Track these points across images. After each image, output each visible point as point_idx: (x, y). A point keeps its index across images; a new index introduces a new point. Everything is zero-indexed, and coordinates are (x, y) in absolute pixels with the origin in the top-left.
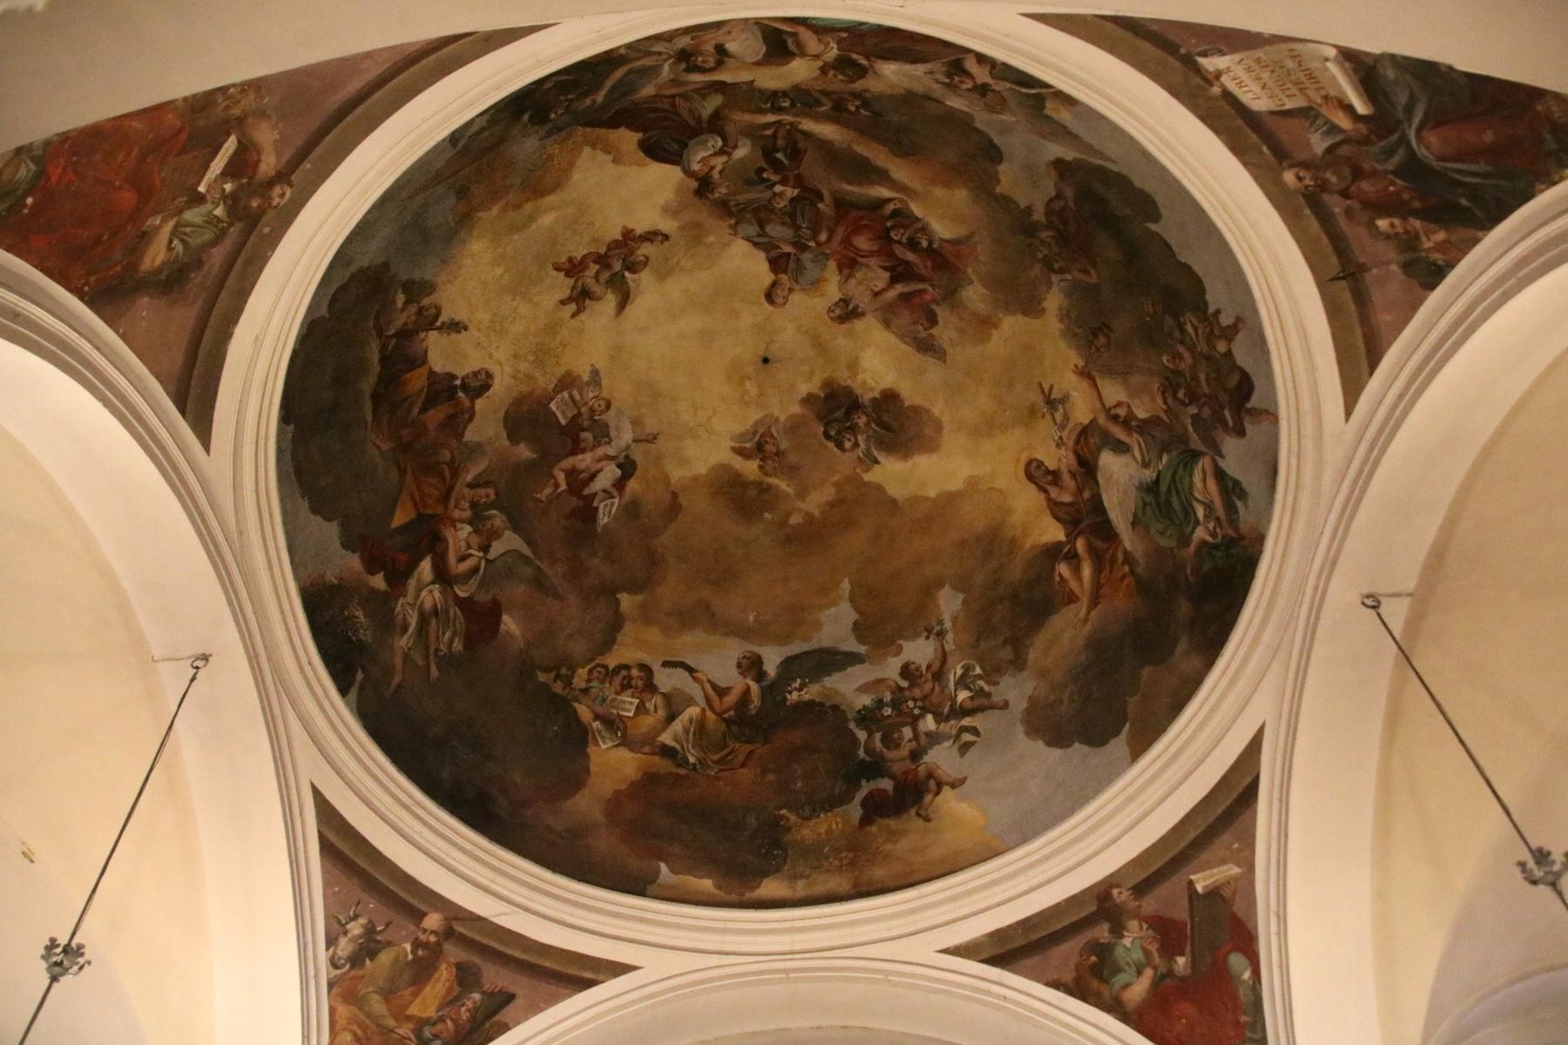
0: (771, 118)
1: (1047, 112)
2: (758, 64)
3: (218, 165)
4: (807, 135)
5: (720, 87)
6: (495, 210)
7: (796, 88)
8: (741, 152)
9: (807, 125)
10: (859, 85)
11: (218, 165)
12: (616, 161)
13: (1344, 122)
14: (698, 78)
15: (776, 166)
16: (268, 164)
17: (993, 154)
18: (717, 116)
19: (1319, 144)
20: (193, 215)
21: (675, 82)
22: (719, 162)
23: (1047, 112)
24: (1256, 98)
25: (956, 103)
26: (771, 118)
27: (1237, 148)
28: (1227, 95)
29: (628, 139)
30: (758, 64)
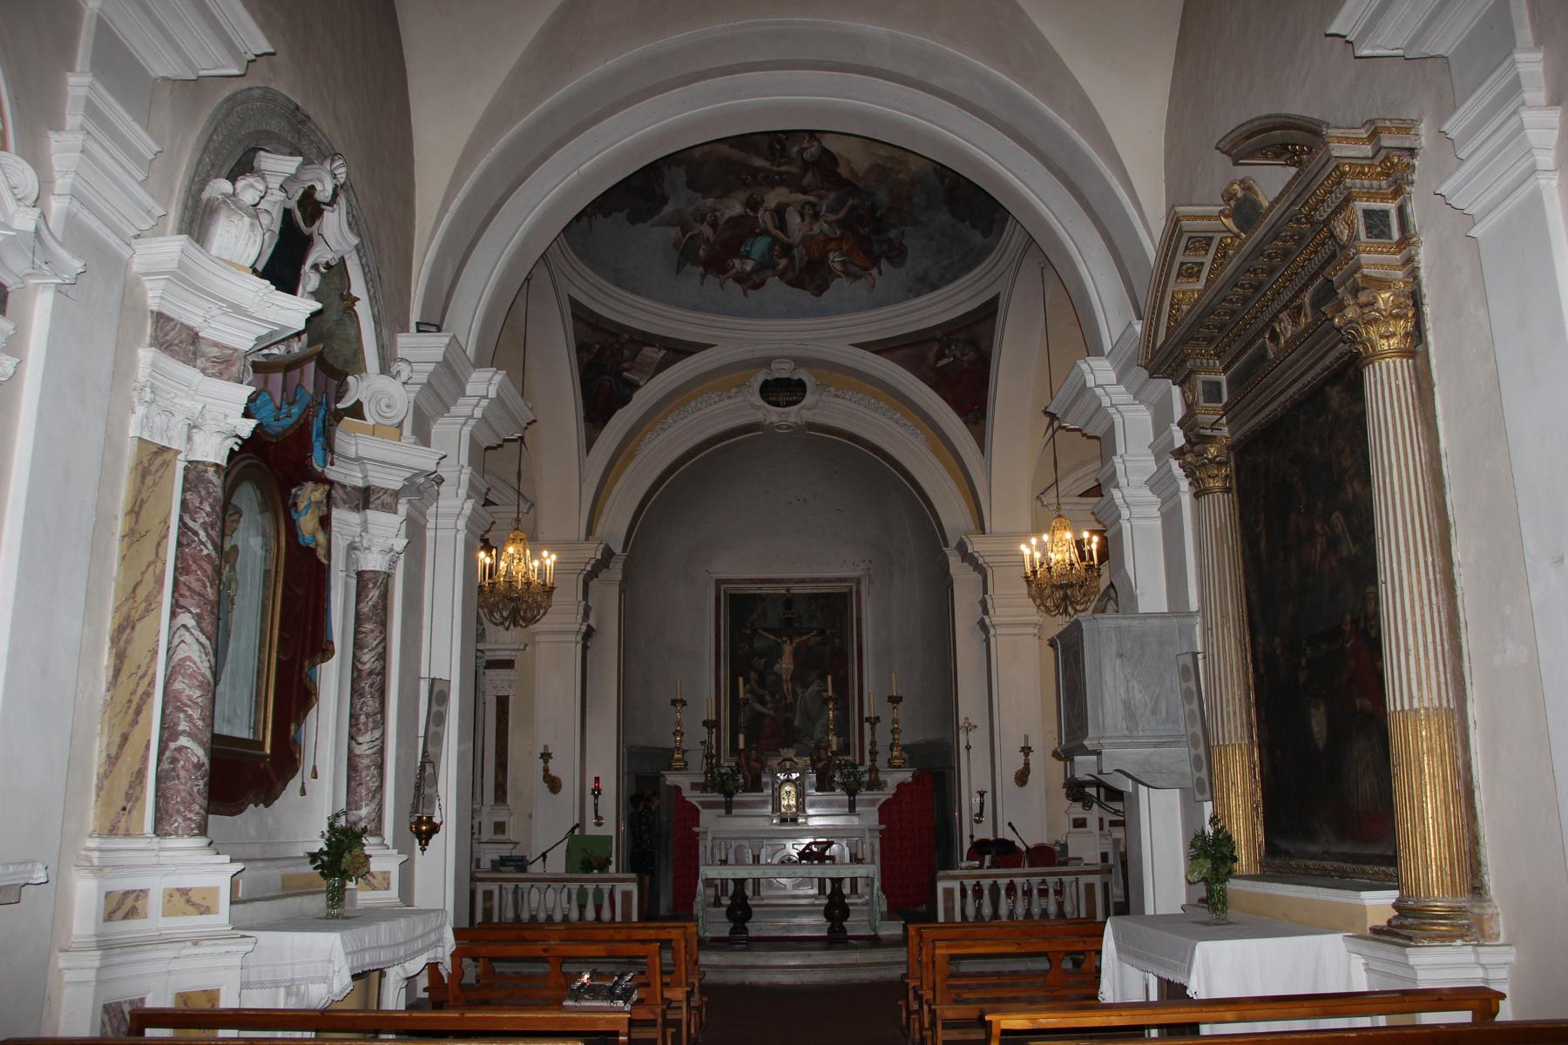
0: (783, 169)
1: (678, 229)
2: (788, 205)
3: (945, 361)
4: (766, 159)
5: (804, 191)
6: (901, 176)
7: (773, 187)
8: (795, 149)
9: (767, 164)
10: (749, 192)
11: (945, 361)
12: (849, 162)
13: (626, 365)
14: (812, 199)
15: (780, 142)
16: (936, 347)
17: (691, 184)
18: (805, 172)
19: (626, 353)
20: (958, 354)
21: (821, 198)
22: (805, 145)
23: (678, 229)
24: (647, 351)
25: (710, 201)
26: (783, 169)
27: (644, 333)
28: (653, 346)
29: (843, 171)
30: (788, 205)
